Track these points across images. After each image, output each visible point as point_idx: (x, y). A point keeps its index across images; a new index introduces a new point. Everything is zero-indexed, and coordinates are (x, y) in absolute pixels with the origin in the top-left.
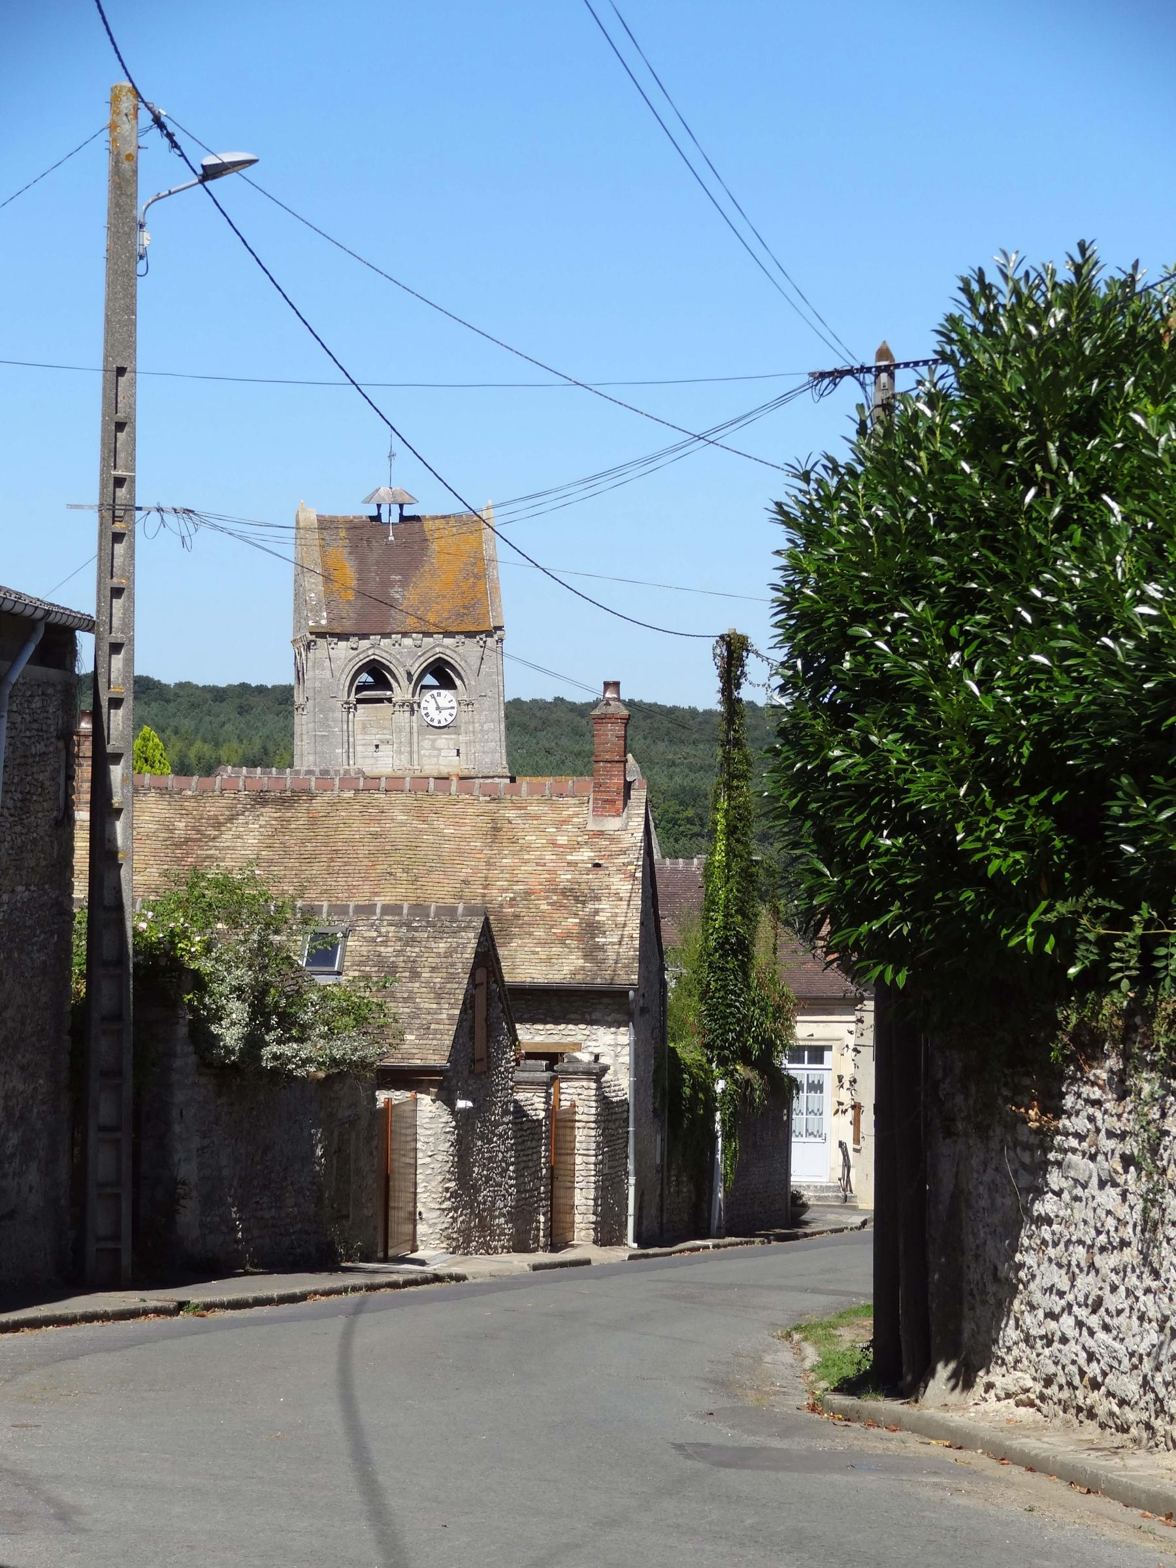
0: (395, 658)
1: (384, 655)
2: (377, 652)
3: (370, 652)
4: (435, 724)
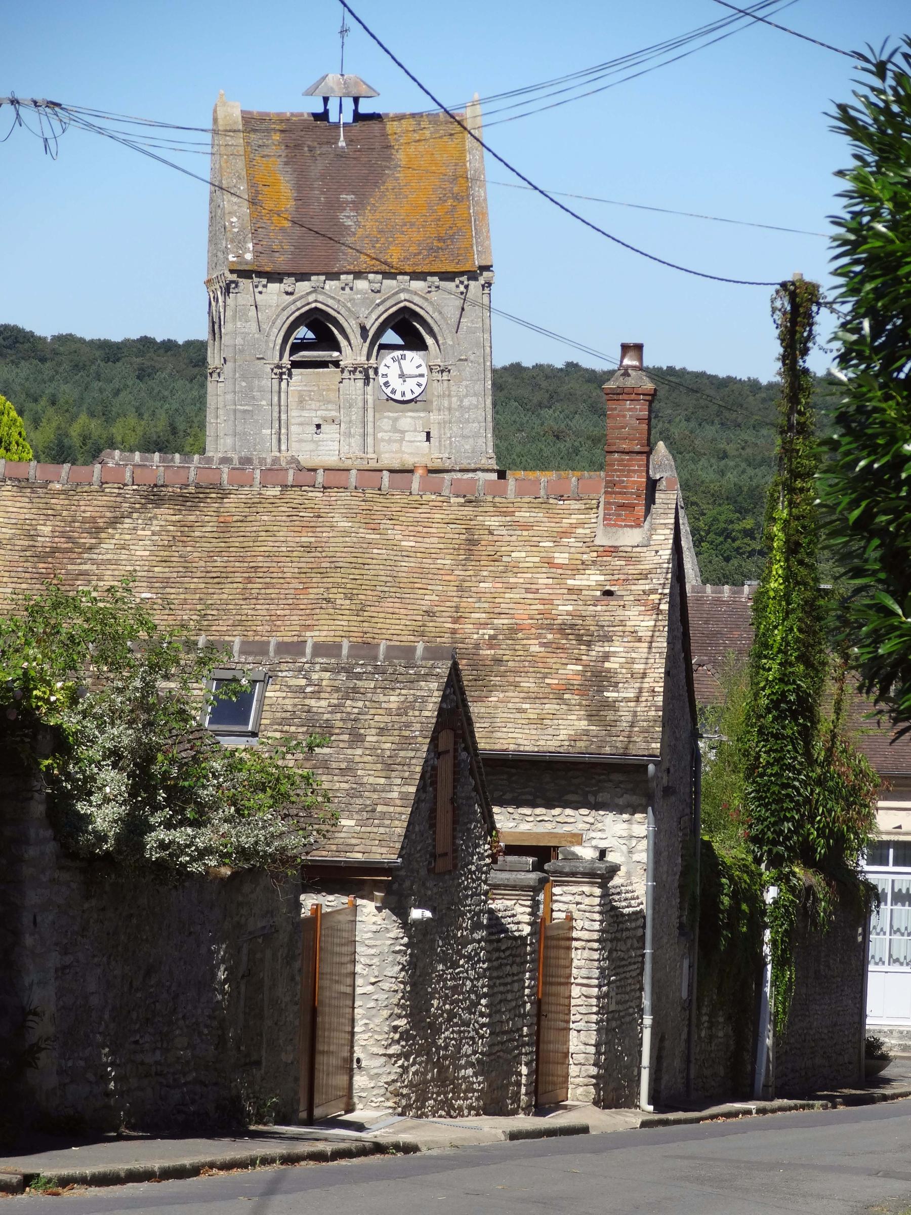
1: (330, 302)
2: (321, 298)
3: (311, 298)
4: (398, 397)
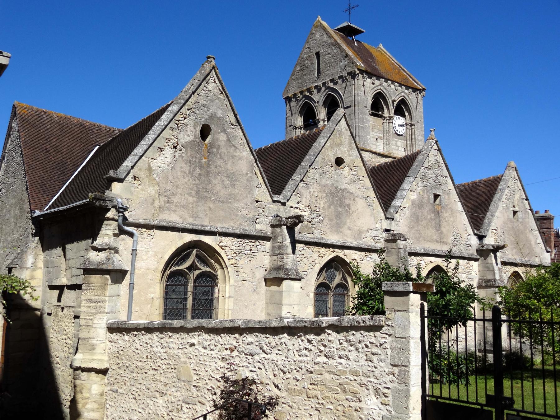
1: (384, 91)
2: (382, 88)
3: (379, 87)
4: (398, 133)
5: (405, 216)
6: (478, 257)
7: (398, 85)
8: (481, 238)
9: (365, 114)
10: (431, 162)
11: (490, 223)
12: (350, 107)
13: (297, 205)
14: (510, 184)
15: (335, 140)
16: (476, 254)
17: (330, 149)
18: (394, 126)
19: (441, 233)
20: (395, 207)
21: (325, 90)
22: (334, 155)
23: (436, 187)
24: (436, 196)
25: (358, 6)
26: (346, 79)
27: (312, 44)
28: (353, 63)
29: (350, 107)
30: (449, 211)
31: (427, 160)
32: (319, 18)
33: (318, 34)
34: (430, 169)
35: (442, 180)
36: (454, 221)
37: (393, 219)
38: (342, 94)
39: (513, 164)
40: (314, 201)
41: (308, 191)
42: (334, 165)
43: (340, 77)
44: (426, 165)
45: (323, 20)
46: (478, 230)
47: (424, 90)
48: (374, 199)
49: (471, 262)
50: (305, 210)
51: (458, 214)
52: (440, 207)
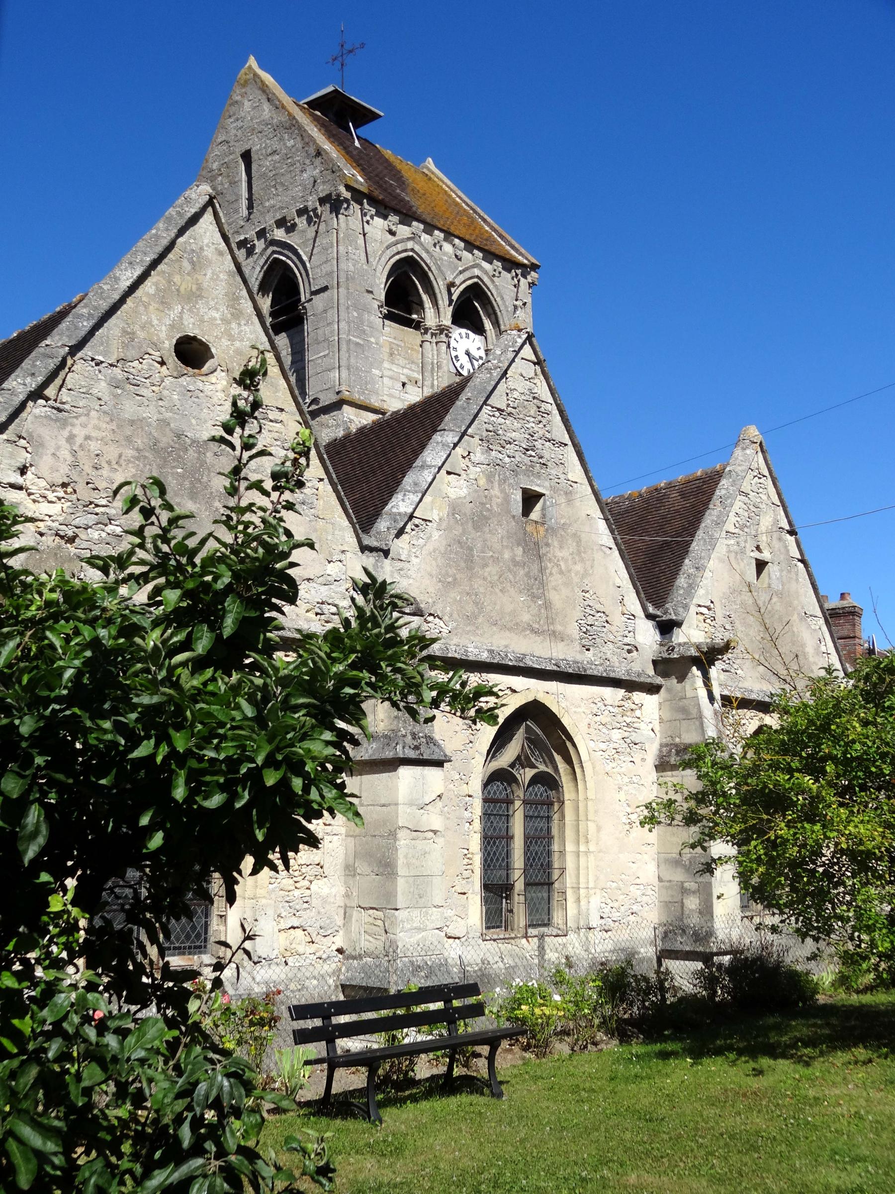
0: (436, 264)
1: (424, 255)
2: (417, 248)
3: (410, 245)
5: (430, 547)
6: (659, 680)
7: (462, 245)
8: (666, 627)
9: (366, 309)
10: (516, 394)
11: (691, 588)
12: (325, 289)
13: (17, 479)
14: (746, 487)
15: (177, 279)
16: (651, 671)
17: (153, 306)
18: (454, 354)
19: (548, 605)
20: (394, 518)
21: (265, 249)
22: (172, 327)
23: (529, 470)
24: (530, 499)
25: (363, 45)
26: (317, 216)
27: (233, 132)
28: (334, 170)
29: (325, 289)
30: (572, 545)
31: (502, 387)
32: (252, 62)
33: (247, 104)
34: (510, 414)
35: (548, 452)
36: (585, 574)
37: (386, 553)
38: (305, 258)
39: (753, 432)
40: (88, 469)
41: (66, 433)
42: (172, 359)
43: (301, 212)
44: (498, 400)
45: (261, 66)
46: (657, 606)
47: (534, 267)
48: (320, 485)
49: (639, 697)
50: (51, 496)
51: (598, 556)
52: (541, 529)
